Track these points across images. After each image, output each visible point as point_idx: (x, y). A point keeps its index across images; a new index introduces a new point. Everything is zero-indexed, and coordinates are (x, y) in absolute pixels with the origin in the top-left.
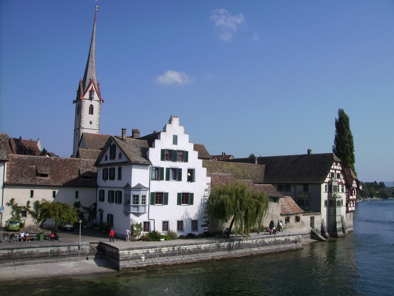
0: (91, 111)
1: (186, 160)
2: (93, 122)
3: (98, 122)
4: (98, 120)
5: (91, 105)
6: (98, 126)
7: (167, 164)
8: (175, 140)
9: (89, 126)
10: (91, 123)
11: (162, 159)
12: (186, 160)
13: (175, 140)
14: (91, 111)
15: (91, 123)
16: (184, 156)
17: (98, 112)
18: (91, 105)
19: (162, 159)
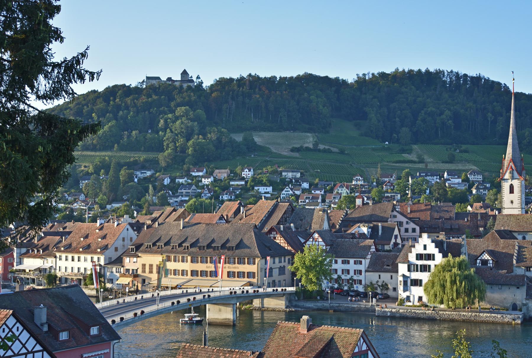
0: (512, 191)
1: (434, 259)
2: (514, 202)
3: (519, 201)
4: (519, 198)
5: (512, 185)
6: (520, 205)
7: (420, 263)
8: (425, 247)
9: (510, 205)
10: (512, 202)
11: (417, 259)
12: (434, 259)
13: (425, 247)
14: (512, 191)
15: (512, 202)
16: (430, 257)
17: (519, 190)
18: (512, 185)
19: (417, 259)
